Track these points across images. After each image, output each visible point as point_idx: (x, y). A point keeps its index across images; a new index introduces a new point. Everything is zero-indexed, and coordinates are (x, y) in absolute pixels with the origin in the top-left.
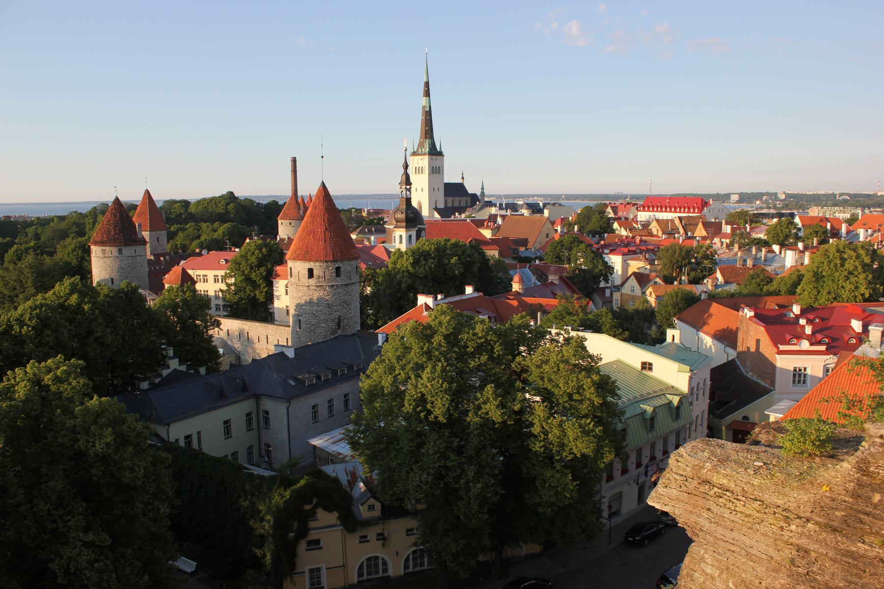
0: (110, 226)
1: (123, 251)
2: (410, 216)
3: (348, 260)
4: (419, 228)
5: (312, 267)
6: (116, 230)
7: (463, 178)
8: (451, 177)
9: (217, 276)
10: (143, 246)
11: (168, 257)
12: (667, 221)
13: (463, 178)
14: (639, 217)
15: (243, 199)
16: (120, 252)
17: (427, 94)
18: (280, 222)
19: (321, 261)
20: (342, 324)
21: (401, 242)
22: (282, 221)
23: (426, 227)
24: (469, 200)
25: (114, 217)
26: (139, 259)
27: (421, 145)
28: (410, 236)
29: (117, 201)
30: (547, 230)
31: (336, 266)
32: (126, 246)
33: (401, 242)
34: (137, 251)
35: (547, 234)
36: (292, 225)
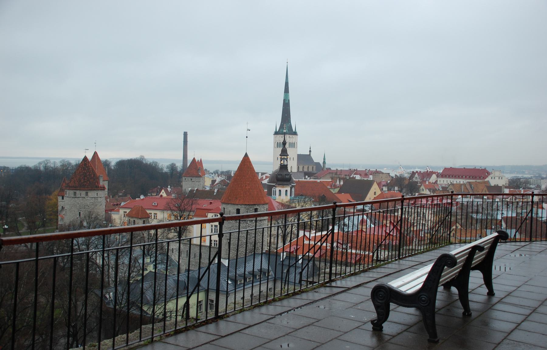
0: (81, 176)
1: (89, 194)
2: (287, 177)
3: (262, 204)
4: (292, 186)
5: (239, 208)
6: (85, 179)
7: (310, 151)
8: (303, 150)
9: (151, 214)
10: (103, 191)
11: (108, 200)
12: (461, 185)
13: (310, 151)
14: (438, 182)
15: (151, 161)
16: (87, 194)
17: (287, 90)
18: (184, 178)
19: (245, 205)
20: (256, 246)
21: (280, 195)
22: (185, 178)
23: (295, 184)
24: (314, 167)
25: (84, 170)
26: (99, 200)
27: (282, 127)
28: (286, 191)
29: (85, 159)
30: (375, 189)
31: (255, 208)
32: (91, 190)
33: (280, 195)
34: (98, 194)
35: (375, 193)
36: (192, 181)
